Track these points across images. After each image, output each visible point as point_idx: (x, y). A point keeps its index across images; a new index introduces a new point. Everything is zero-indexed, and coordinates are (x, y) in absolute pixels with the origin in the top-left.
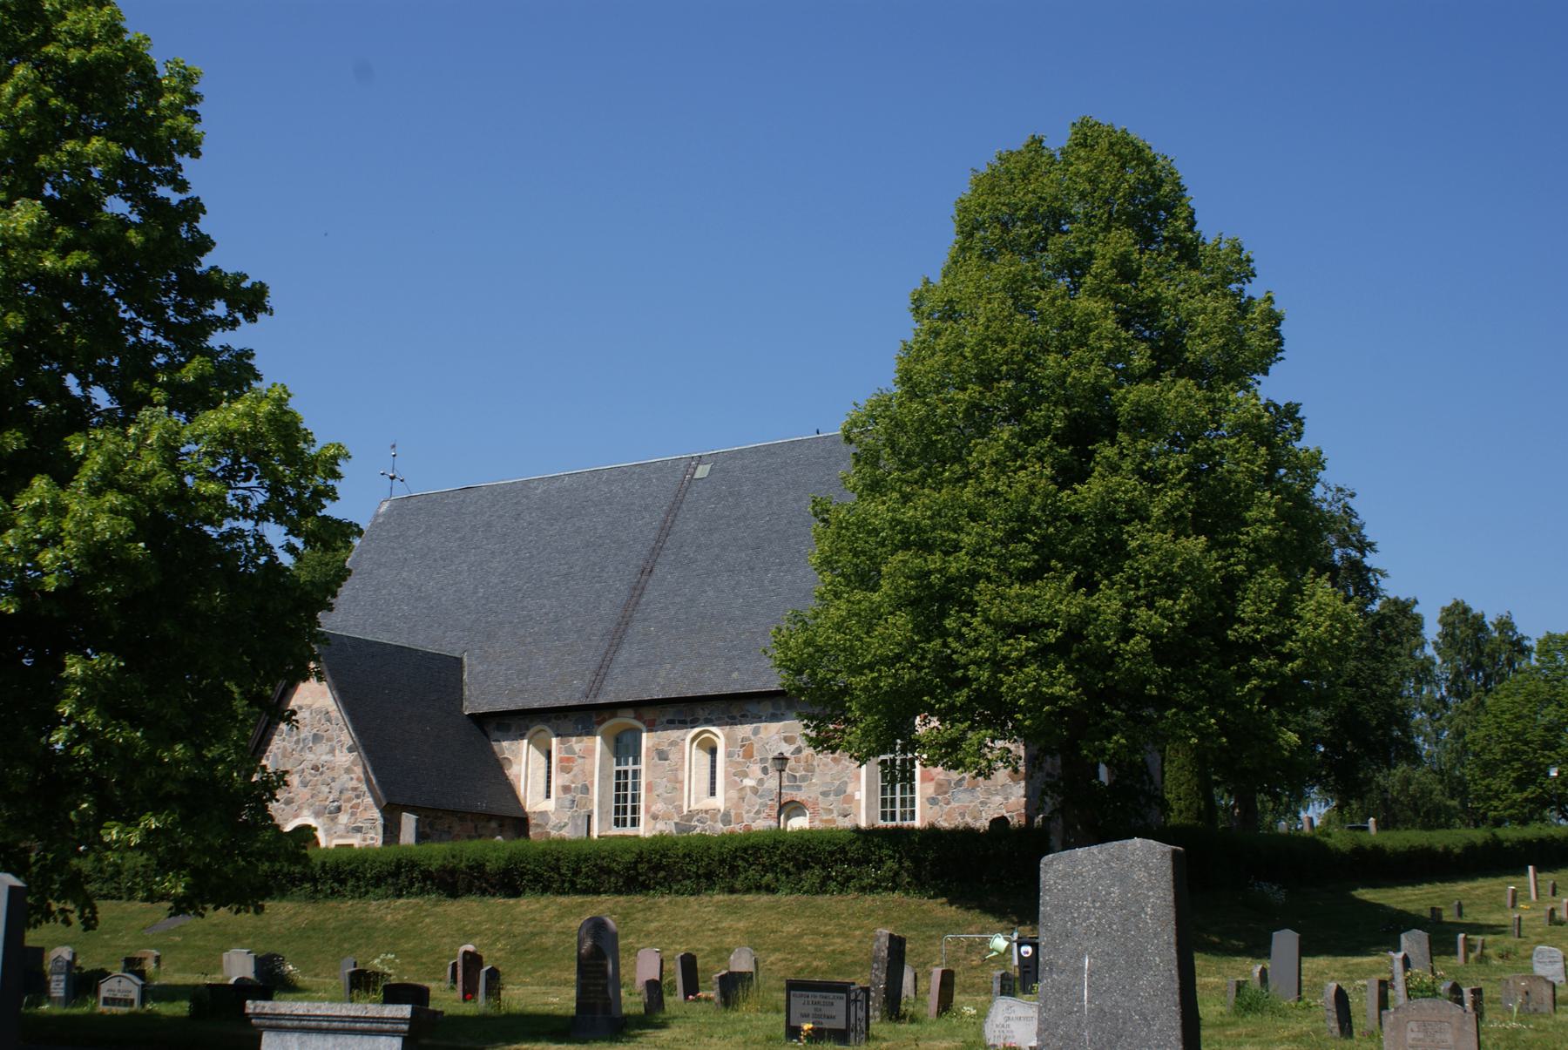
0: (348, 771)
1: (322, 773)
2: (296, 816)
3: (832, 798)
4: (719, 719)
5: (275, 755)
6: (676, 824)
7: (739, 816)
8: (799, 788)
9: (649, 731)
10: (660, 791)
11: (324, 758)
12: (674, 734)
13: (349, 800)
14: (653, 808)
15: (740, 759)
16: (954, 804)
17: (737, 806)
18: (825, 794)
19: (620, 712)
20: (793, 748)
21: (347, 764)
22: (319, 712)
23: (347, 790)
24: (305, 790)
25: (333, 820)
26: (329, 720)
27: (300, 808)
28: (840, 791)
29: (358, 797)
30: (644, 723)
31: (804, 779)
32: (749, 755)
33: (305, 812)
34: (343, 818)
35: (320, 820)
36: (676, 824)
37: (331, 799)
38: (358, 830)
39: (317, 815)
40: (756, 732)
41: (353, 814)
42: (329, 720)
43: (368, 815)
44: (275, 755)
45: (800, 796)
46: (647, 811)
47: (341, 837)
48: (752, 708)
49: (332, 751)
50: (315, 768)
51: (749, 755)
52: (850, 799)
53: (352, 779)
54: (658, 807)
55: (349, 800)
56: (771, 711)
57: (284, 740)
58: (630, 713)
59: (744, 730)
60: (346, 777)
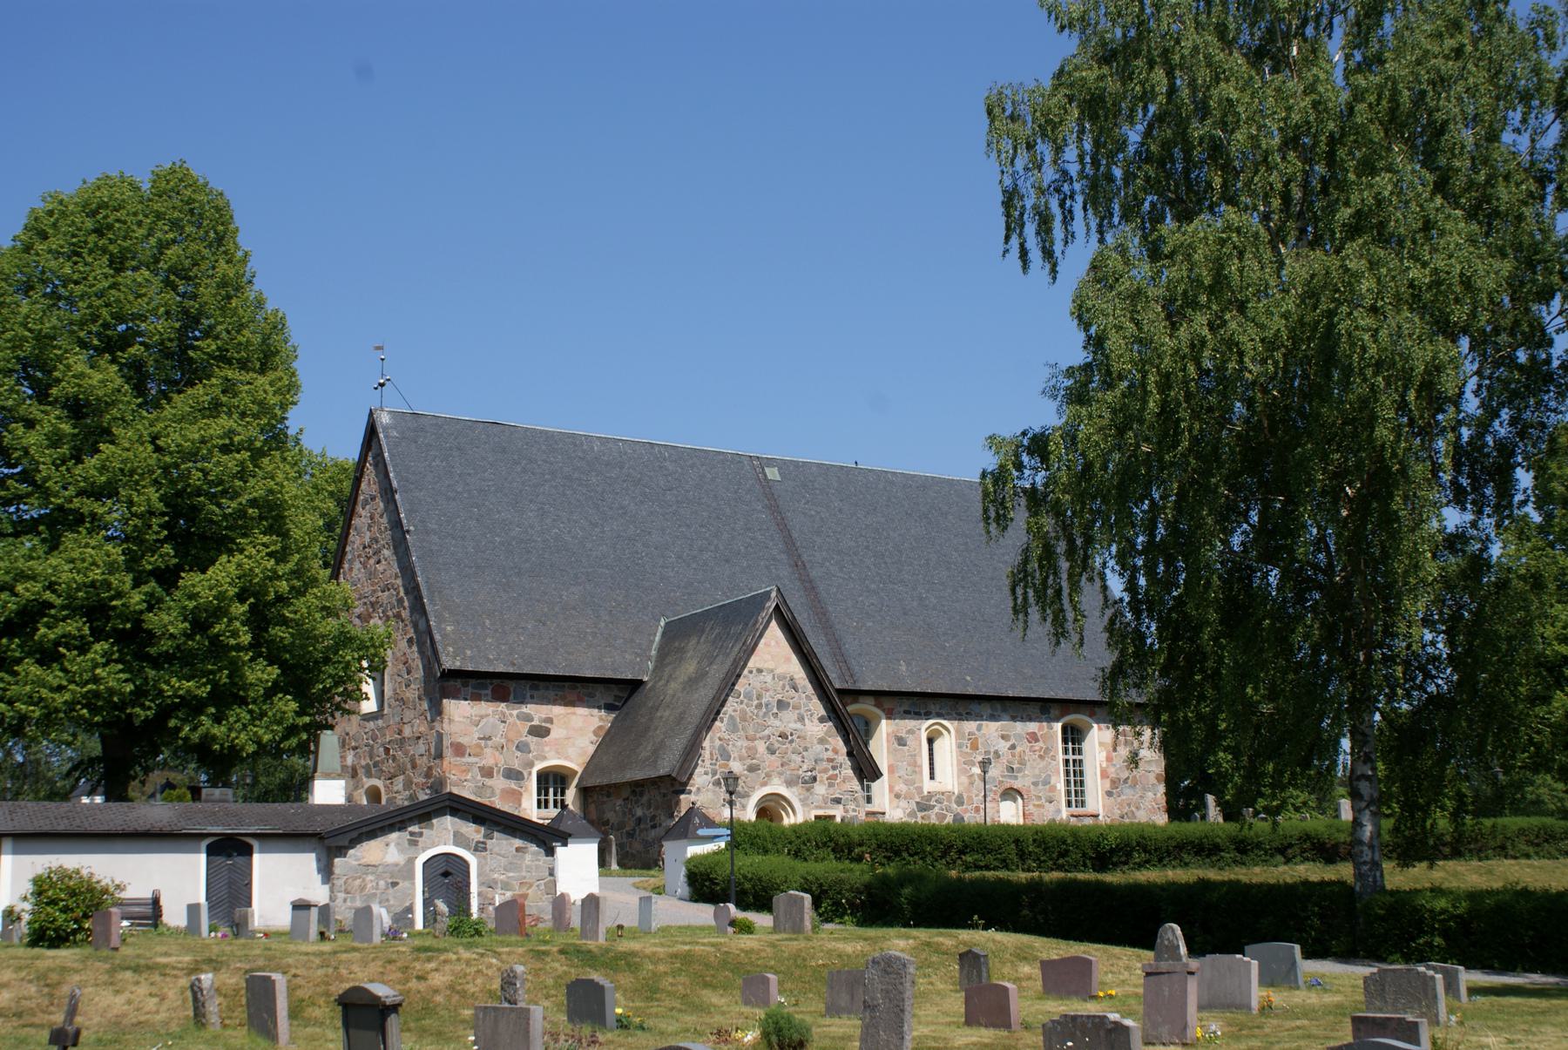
0: (822, 741)
1: (792, 741)
2: (764, 784)
3: (1040, 787)
4: (948, 714)
5: (731, 717)
6: (917, 803)
7: (970, 798)
8: (1016, 778)
9: (888, 718)
10: (902, 773)
11: (793, 725)
12: (910, 724)
13: (825, 771)
14: (897, 788)
15: (968, 750)
16: (1123, 797)
17: (969, 791)
18: (1035, 784)
19: (861, 698)
20: (1008, 744)
21: (821, 734)
22: (782, 677)
23: (822, 760)
24: (773, 757)
25: (808, 790)
26: (795, 688)
27: (768, 775)
28: (1046, 782)
29: (834, 768)
30: (883, 710)
31: (1020, 770)
32: (975, 747)
33: (776, 780)
34: (820, 789)
35: (794, 789)
36: (917, 803)
37: (805, 767)
38: (838, 801)
39: (789, 783)
40: (979, 728)
41: (831, 785)
42: (795, 688)
43: (847, 786)
44: (731, 717)
45: (1017, 785)
46: (891, 789)
47: (820, 808)
48: (974, 707)
49: (801, 719)
50: (783, 736)
51: (975, 747)
52: (1053, 789)
53: (827, 750)
54: (901, 787)
55: (825, 771)
56: (989, 711)
57: (742, 702)
58: (871, 700)
59: (970, 726)
60: (819, 748)
